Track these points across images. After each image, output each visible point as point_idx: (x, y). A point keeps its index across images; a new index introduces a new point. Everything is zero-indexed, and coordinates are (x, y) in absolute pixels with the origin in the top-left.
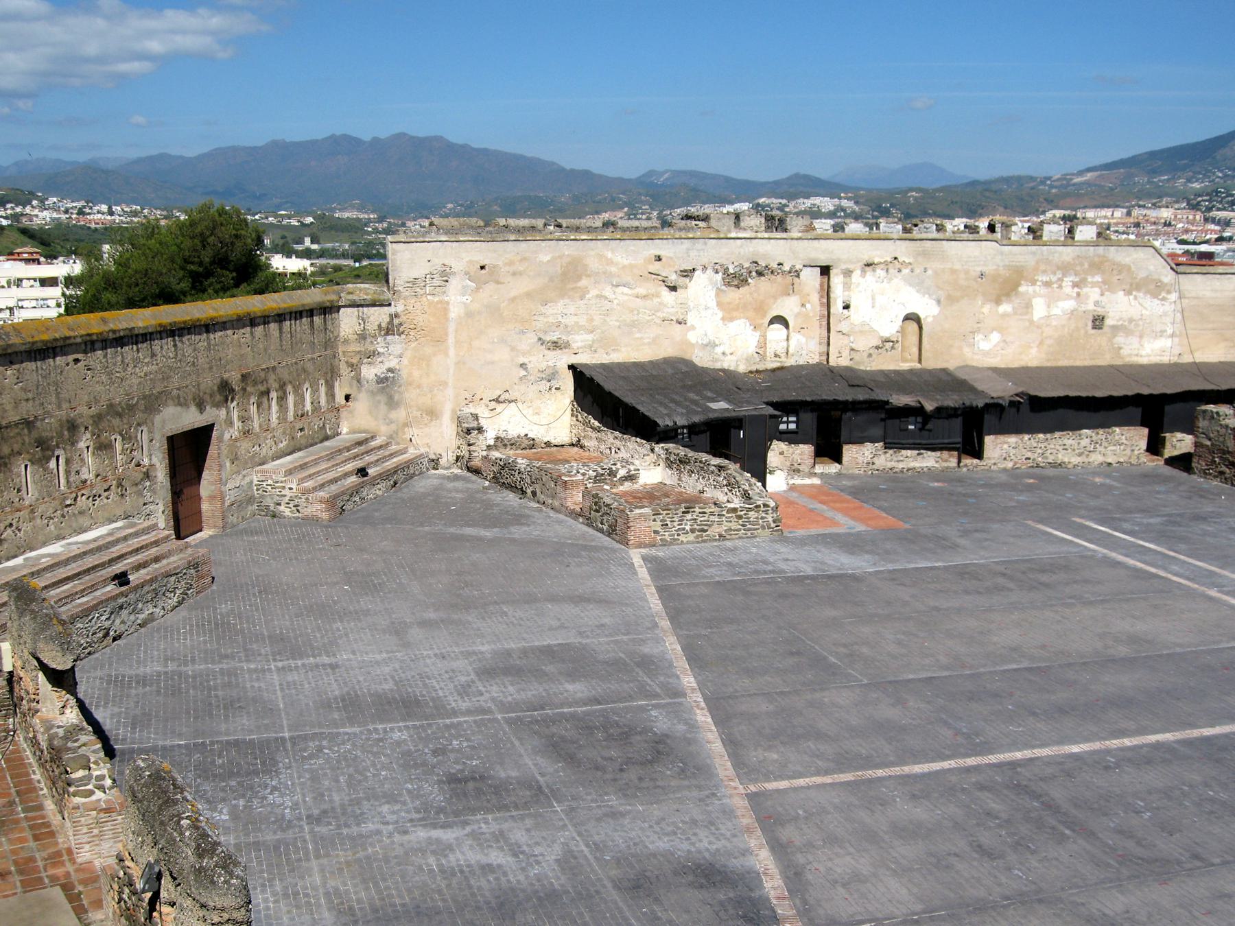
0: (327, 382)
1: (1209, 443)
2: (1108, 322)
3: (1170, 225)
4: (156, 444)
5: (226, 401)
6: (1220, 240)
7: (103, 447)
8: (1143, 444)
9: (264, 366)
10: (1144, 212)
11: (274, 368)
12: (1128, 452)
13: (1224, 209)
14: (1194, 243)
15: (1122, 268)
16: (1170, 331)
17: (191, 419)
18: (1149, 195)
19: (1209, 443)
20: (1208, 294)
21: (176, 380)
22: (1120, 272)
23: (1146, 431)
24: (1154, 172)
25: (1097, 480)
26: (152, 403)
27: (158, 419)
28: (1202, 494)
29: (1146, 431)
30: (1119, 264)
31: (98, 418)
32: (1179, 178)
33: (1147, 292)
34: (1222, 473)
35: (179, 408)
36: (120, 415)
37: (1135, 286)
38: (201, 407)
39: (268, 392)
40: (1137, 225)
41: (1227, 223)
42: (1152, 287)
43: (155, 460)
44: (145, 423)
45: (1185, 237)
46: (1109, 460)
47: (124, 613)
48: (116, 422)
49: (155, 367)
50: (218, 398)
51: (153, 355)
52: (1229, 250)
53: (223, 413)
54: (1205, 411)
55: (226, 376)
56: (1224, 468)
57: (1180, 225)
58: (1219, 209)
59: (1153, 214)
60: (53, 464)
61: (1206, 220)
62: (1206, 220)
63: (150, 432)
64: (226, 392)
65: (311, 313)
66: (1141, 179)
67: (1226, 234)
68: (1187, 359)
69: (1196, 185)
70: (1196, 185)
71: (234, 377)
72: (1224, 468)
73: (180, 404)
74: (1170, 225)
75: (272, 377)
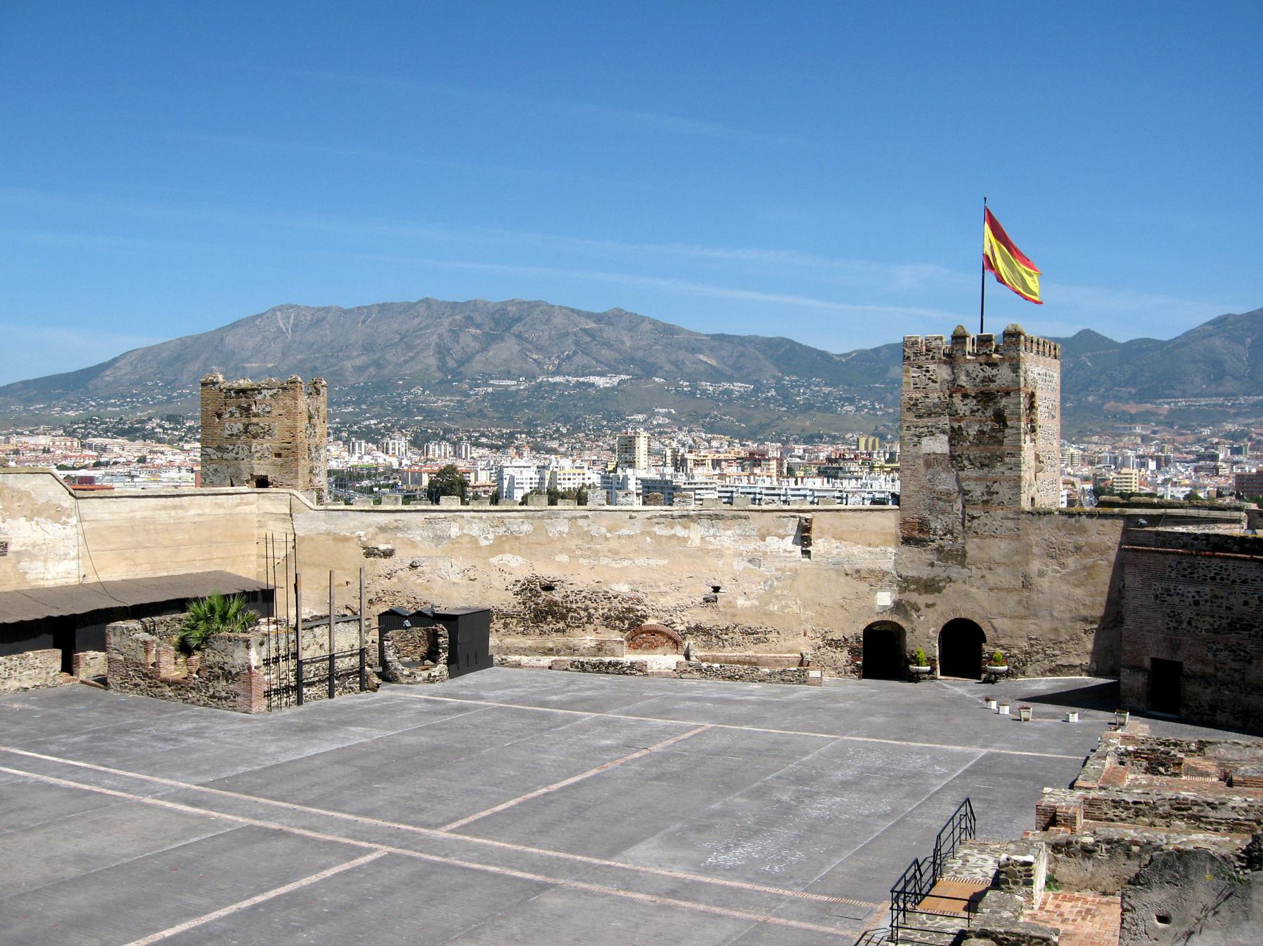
1: (121, 658)
2: (11, 548)
3: (49, 451)
6: (98, 465)
8: (58, 665)
10: (24, 439)
12: (44, 675)
13: (100, 436)
14: (73, 468)
15: (20, 495)
16: (73, 553)
18: (27, 423)
19: (121, 658)
20: (107, 516)
22: (20, 499)
23: (59, 652)
24: (30, 401)
25: (16, 706)
28: (122, 707)
29: (59, 652)
30: (18, 491)
32: (55, 406)
33: (48, 517)
34: (136, 685)
37: (34, 513)
40: (16, 452)
41: (104, 449)
42: (53, 512)
45: (64, 463)
46: (25, 686)
52: (107, 474)
54: (114, 628)
56: (138, 681)
57: (59, 452)
58: (94, 436)
59: (32, 441)
61: (83, 446)
62: (83, 446)
67: (102, 460)
68: (92, 579)
69: (71, 413)
70: (71, 413)
72: (138, 681)
74: (49, 451)
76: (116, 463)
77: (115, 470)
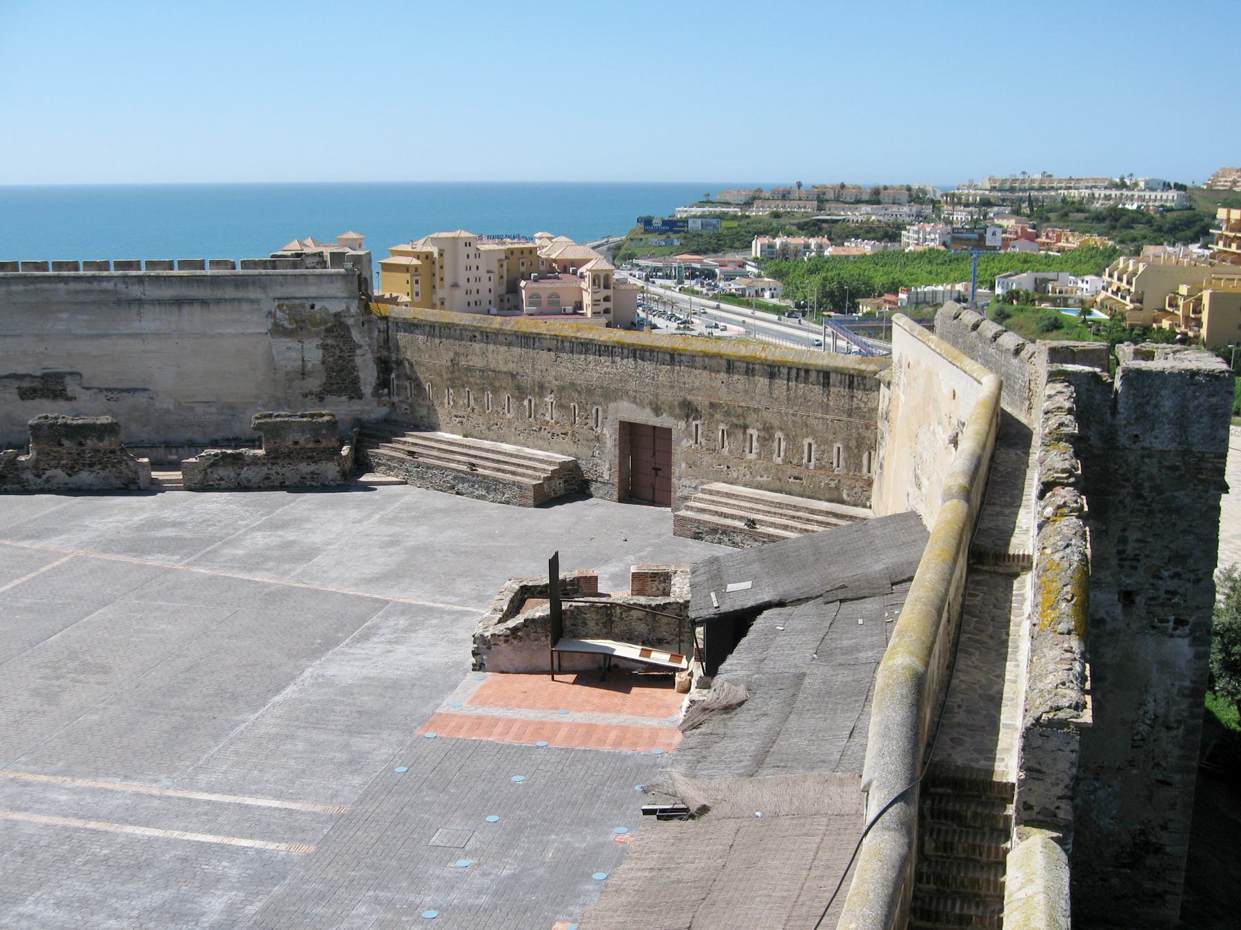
0: (847, 448)
4: (609, 422)
5: (688, 417)
7: (561, 406)
9: (743, 404)
11: (756, 410)
17: (644, 416)
21: (632, 385)
26: (610, 395)
27: (612, 405)
31: (562, 389)
35: (634, 406)
36: (579, 393)
38: (657, 411)
39: (745, 427)
43: (605, 431)
44: (600, 404)
47: (466, 485)
48: (575, 395)
49: (614, 370)
50: (677, 411)
51: (613, 362)
53: (682, 424)
55: (689, 398)
60: (526, 403)
63: (605, 412)
64: (689, 410)
65: (825, 376)
71: (700, 400)
73: (634, 402)
75: (751, 418)
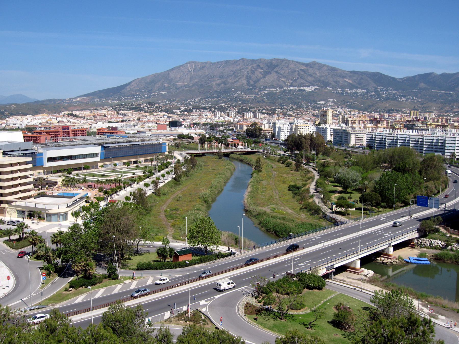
3: (106, 116)
6: (123, 121)
10: (97, 111)
13: (125, 110)
14: (114, 122)
40: (94, 116)
41: (125, 115)
45: (111, 120)
52: (126, 125)
57: (109, 116)
58: (123, 110)
61: (118, 114)
62: (118, 114)
66: (97, 100)
67: (124, 119)
74: (106, 116)
76: (129, 120)
77: (129, 123)
